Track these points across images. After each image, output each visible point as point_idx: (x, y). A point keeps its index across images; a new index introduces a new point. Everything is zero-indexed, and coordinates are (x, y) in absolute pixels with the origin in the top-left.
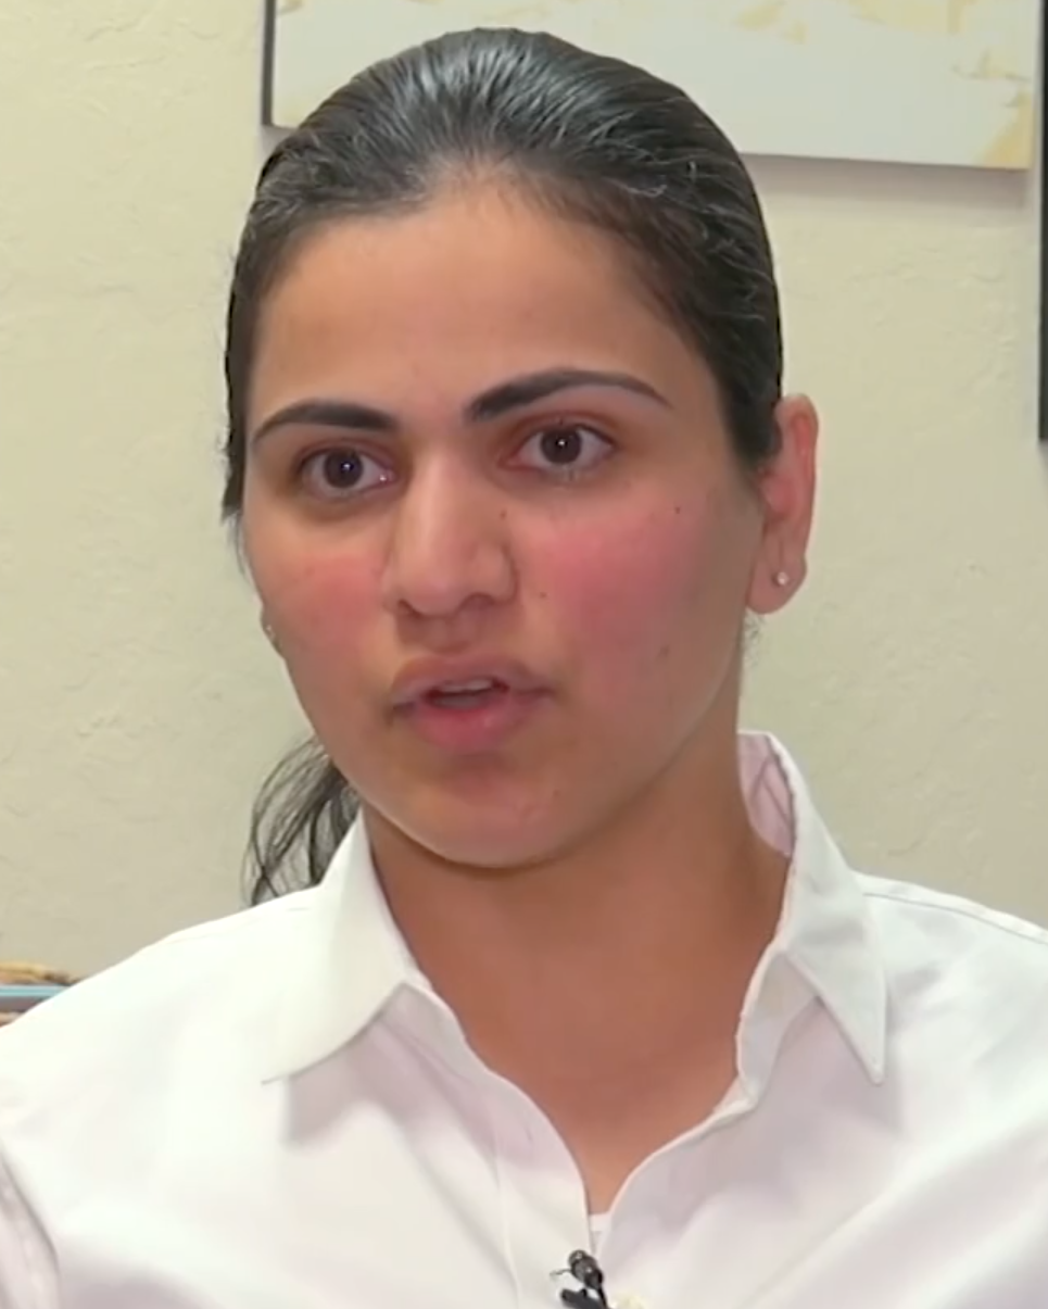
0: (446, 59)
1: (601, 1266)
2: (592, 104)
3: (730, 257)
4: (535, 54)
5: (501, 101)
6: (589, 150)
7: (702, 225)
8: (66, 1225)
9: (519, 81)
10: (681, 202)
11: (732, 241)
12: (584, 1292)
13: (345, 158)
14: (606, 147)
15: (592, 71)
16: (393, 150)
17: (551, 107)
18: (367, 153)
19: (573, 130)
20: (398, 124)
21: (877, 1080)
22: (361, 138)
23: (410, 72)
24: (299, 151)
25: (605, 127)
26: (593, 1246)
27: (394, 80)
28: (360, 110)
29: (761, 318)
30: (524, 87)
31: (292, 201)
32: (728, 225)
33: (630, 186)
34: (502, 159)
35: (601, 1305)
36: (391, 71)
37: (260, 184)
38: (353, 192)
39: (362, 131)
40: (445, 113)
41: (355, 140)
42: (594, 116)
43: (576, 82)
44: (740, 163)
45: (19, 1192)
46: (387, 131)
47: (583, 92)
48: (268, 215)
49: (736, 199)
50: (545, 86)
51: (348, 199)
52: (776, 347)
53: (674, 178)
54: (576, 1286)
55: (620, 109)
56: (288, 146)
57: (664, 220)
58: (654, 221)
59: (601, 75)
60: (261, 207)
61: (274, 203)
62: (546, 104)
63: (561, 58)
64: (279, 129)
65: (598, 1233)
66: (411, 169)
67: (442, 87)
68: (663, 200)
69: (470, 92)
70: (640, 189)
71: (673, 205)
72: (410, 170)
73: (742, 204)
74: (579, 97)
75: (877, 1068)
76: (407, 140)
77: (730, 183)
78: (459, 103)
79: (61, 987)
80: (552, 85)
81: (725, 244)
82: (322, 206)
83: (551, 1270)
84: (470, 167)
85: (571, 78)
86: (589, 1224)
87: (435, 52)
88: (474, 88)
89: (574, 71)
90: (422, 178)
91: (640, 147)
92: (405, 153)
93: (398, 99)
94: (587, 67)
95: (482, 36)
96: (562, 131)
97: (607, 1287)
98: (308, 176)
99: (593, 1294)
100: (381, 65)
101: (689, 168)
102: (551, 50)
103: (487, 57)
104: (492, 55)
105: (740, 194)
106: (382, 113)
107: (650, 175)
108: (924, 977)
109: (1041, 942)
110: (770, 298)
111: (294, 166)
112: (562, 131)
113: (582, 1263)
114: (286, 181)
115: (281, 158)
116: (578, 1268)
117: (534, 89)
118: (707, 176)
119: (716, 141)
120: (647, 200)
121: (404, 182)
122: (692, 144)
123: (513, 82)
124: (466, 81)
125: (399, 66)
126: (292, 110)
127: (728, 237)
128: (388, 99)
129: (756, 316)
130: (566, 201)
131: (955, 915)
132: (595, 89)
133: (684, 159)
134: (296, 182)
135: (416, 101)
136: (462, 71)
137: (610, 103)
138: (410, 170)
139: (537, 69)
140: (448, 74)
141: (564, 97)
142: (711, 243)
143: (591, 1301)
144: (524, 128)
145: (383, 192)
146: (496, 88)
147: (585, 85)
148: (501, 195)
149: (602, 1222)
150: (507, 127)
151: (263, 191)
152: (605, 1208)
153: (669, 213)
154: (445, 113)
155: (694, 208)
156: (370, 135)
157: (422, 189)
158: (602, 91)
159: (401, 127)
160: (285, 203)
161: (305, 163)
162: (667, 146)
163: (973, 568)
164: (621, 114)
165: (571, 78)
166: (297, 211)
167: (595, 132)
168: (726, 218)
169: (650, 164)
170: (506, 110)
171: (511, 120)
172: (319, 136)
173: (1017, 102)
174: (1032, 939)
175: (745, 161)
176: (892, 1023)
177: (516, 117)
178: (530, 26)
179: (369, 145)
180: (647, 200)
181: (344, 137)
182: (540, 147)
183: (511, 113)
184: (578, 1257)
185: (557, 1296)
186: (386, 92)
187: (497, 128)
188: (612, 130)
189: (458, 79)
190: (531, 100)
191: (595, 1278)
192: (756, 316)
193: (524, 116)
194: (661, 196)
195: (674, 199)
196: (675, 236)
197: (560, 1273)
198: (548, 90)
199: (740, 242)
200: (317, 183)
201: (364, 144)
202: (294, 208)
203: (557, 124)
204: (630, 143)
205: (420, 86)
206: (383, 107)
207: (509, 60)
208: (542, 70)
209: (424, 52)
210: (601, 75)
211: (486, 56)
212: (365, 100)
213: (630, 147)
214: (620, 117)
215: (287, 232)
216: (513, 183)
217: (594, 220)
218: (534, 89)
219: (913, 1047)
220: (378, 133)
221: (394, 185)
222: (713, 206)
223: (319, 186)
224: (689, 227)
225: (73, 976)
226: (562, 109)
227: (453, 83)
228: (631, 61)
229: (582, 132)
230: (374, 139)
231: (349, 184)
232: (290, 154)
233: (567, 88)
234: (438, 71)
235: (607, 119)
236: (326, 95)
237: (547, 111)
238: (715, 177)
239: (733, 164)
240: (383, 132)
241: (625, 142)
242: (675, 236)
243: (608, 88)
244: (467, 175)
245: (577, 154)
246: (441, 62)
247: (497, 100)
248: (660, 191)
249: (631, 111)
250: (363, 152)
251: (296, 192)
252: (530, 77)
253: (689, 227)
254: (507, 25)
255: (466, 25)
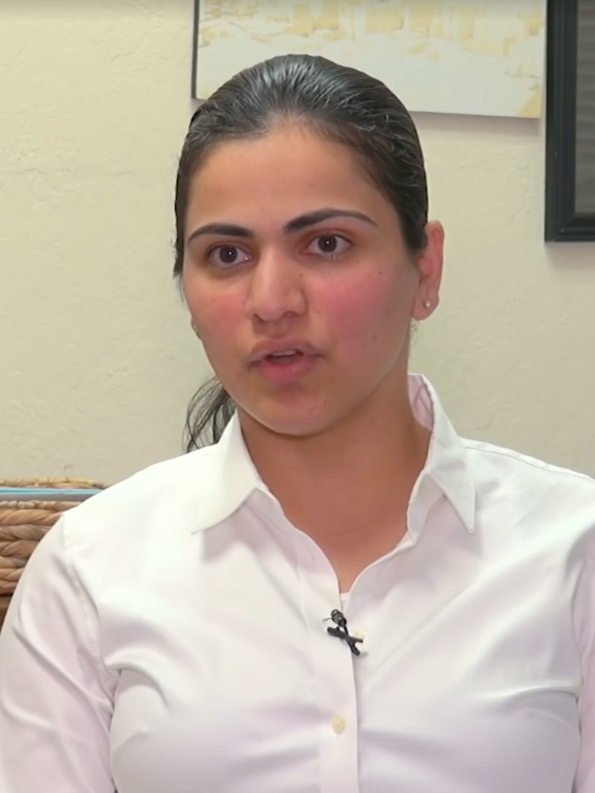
0: (275, 68)
1: (346, 617)
2: (341, 89)
3: (404, 158)
4: (315, 66)
5: (300, 87)
6: (340, 110)
7: (392, 144)
8: (103, 598)
9: (308, 78)
10: (382, 133)
11: (405, 151)
12: (338, 628)
13: (229, 113)
14: (348, 108)
15: (341, 74)
16: (251, 109)
17: (323, 90)
18: (239, 111)
19: (333, 101)
20: (253, 98)
21: (471, 532)
22: (236, 104)
23: (259, 74)
24: (208, 110)
25: (348, 99)
26: (342, 607)
27: (252, 78)
28: (236, 92)
29: (418, 186)
30: (311, 81)
31: (205, 133)
32: (403, 144)
33: (359, 126)
34: (300, 114)
35: (346, 634)
36: (250, 74)
37: (191, 125)
38: (233, 129)
39: (237, 101)
40: (275, 93)
41: (234, 105)
42: (342, 94)
43: (334, 79)
44: (409, 115)
45: (81, 583)
46: (248, 101)
47: (337, 83)
48: (194, 139)
49: (407, 132)
50: (320, 81)
51: (230, 132)
52: (425, 199)
53: (379, 122)
54: (334, 626)
55: (354, 91)
56: (203, 108)
57: (374, 142)
58: (370, 142)
59: (345, 76)
60: (191, 135)
61: (197, 134)
62: (320, 89)
63: (327, 68)
64: (199, 100)
65: (344, 602)
66: (259, 118)
67: (273, 81)
68: (374, 133)
69: (286, 83)
70: (363, 127)
71: (378, 135)
72: (259, 119)
73: (410, 134)
74: (335, 86)
75: (471, 526)
76: (257, 105)
77: (404, 124)
78: (281, 88)
79: (100, 490)
80: (323, 80)
81: (402, 152)
82: (219, 135)
83: (323, 618)
84: (286, 117)
85: (332, 77)
86: (340, 597)
87: (270, 65)
88: (288, 81)
89: (333, 74)
90: (264, 122)
91: (363, 108)
92: (256, 111)
93: (253, 86)
94: (339, 72)
95: (291, 58)
96: (328, 101)
97: (348, 626)
98: (212, 121)
99: (342, 629)
100: (246, 71)
101: (385, 118)
102: (323, 64)
103: (294, 67)
104: (296, 67)
105: (409, 130)
106: (246, 93)
107: (368, 121)
108: (492, 486)
109: (545, 469)
110: (422, 177)
111: (206, 117)
112: (328, 101)
113: (337, 615)
114: (202, 124)
115: (200, 113)
116: (335, 617)
117: (315, 82)
118: (394, 121)
119: (398, 106)
120: (366, 132)
121: (256, 124)
122: (387, 107)
123: (306, 79)
124: (284, 78)
125: (254, 71)
126: (206, 91)
127: (403, 149)
128: (249, 87)
129: (416, 185)
130: (330, 133)
131: (506, 457)
132: (343, 82)
133: (383, 114)
134: (207, 124)
135: (262, 87)
136: (282, 74)
137: (350, 88)
138: (259, 119)
139: (317, 73)
140: (276, 75)
141: (329, 86)
142: (396, 152)
143: (341, 632)
144: (310, 100)
145: (246, 129)
146: (298, 81)
147: (338, 80)
148: (300, 130)
149: (346, 597)
150: (303, 99)
151: (192, 128)
152: (348, 590)
153: (376, 138)
154: (275, 93)
155: (388, 136)
156: (240, 103)
157: (264, 127)
158: (346, 83)
159: (254, 99)
160: (202, 134)
161: (211, 116)
162: (375, 108)
163: (514, 299)
164: (354, 93)
165: (332, 77)
166: (208, 137)
167: (343, 102)
168: (402, 141)
169: (368, 116)
170: (303, 91)
171: (305, 96)
172: (218, 103)
173: (535, 88)
174: (541, 468)
175: (411, 115)
176: (478, 506)
177: (307, 95)
178: (313, 53)
179: (240, 107)
180: (366, 133)
181: (229, 104)
182: (318, 108)
183: (305, 93)
184: (335, 613)
185: (325, 630)
186: (248, 83)
187: (299, 100)
188: (350, 100)
189: (281, 78)
190: (314, 87)
191: (343, 622)
192: (416, 185)
193: (311, 94)
194: (373, 130)
195: (379, 132)
196: (379, 149)
197: (327, 620)
198: (321, 82)
199: (408, 152)
200: (216, 124)
201: (238, 107)
202: (206, 136)
203: (326, 98)
204: (359, 106)
205: (264, 81)
206: (246, 90)
207: (304, 69)
208: (319, 73)
209: (265, 65)
210: (345, 76)
211: (293, 67)
212: (238, 87)
213: (359, 108)
214: (354, 95)
215: (203, 147)
216: (306, 125)
217: (342, 141)
218: (315, 82)
219: (487, 517)
220: (244, 102)
221: (252, 125)
222: (397, 135)
223: (217, 126)
224: (385, 145)
225: (106, 485)
226: (328, 91)
227: (278, 79)
228: (359, 69)
229: (337, 102)
230: (243, 105)
231: (231, 125)
232: (204, 112)
233: (330, 81)
234: (272, 74)
235: (348, 95)
236: (221, 84)
237: (321, 92)
238: (397, 122)
239: (406, 116)
240: (246, 101)
241: (356, 106)
242: (379, 149)
243: (349, 82)
244: (285, 121)
245: (335, 112)
246: (273, 70)
247: (298, 87)
248: (372, 128)
249: (359, 92)
250: (237, 111)
251: (207, 129)
252: (313, 76)
253: (385, 145)
254: (303, 53)
255: (284, 53)
